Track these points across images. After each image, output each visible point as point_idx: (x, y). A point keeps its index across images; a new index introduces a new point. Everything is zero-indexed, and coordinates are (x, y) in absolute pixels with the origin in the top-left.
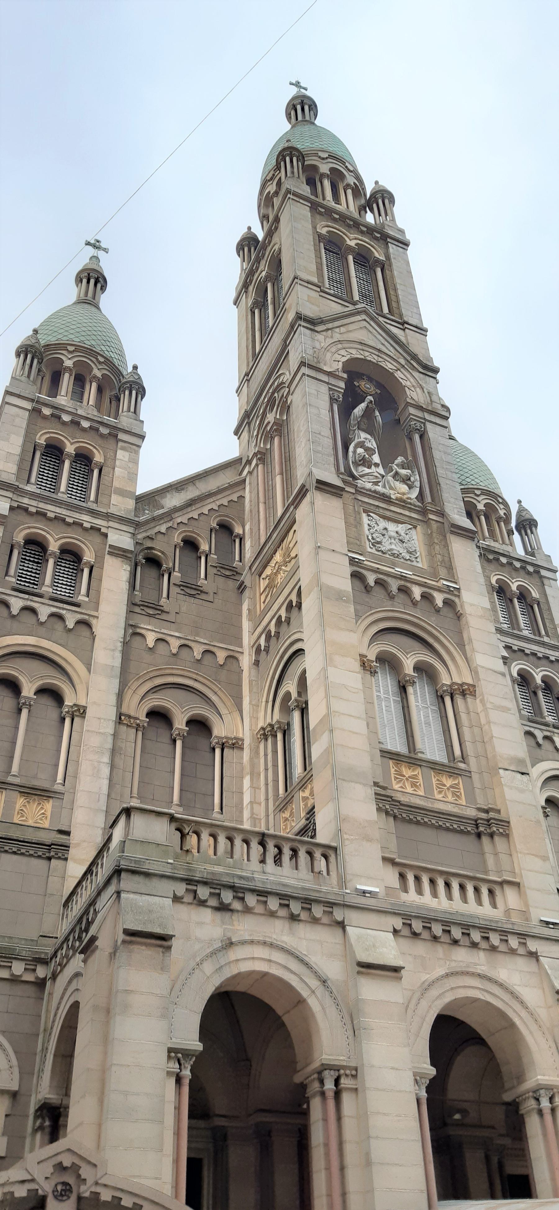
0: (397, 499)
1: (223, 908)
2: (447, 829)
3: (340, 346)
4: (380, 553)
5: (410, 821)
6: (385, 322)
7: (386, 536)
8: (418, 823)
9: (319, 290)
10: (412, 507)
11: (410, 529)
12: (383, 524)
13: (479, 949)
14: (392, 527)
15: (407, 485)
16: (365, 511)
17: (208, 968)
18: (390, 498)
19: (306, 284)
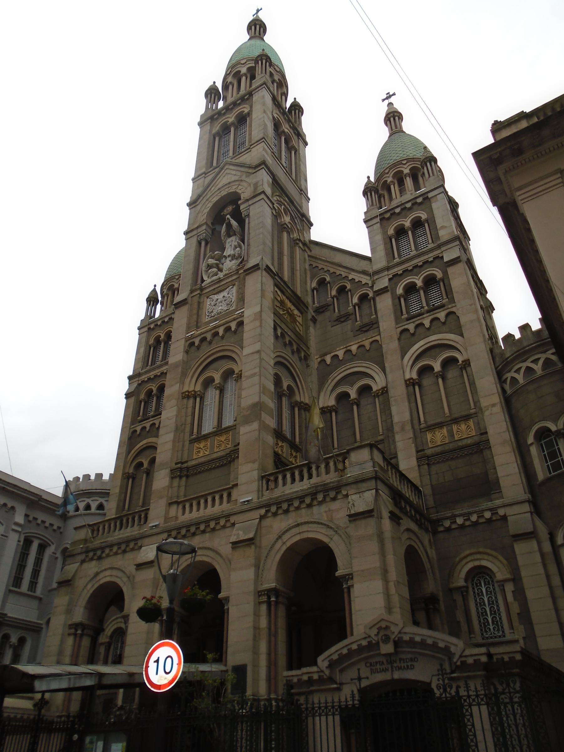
0: (224, 276)
1: (100, 558)
2: (215, 468)
3: (208, 202)
4: (212, 318)
5: (196, 474)
6: (235, 160)
7: (217, 304)
8: (200, 473)
9: (204, 175)
10: (232, 274)
11: (232, 288)
12: (216, 297)
13: (207, 533)
14: (220, 296)
15: (237, 259)
16: (208, 298)
17: (89, 586)
18: (220, 278)
19: (197, 179)
